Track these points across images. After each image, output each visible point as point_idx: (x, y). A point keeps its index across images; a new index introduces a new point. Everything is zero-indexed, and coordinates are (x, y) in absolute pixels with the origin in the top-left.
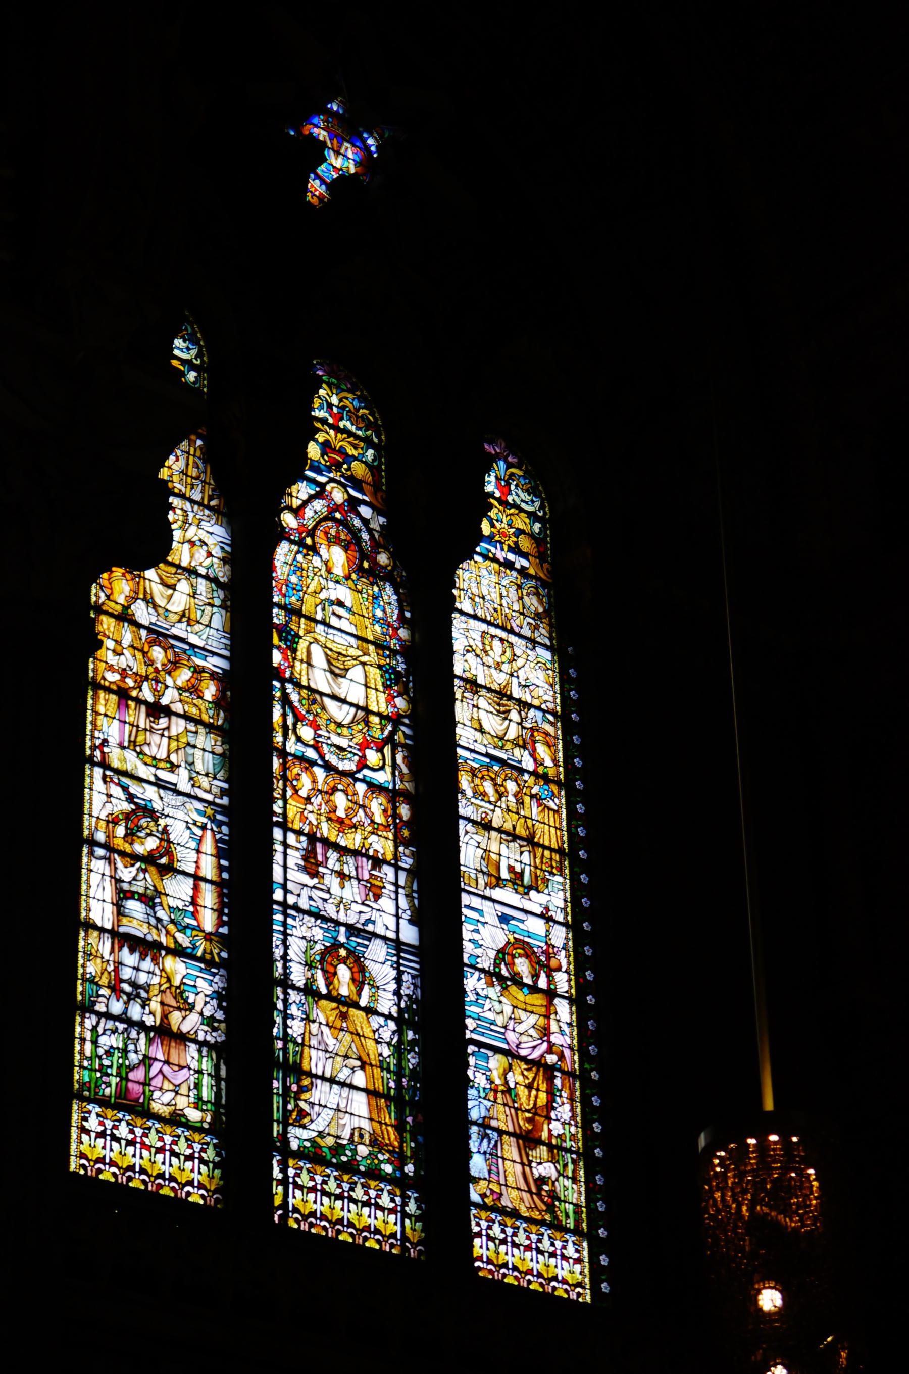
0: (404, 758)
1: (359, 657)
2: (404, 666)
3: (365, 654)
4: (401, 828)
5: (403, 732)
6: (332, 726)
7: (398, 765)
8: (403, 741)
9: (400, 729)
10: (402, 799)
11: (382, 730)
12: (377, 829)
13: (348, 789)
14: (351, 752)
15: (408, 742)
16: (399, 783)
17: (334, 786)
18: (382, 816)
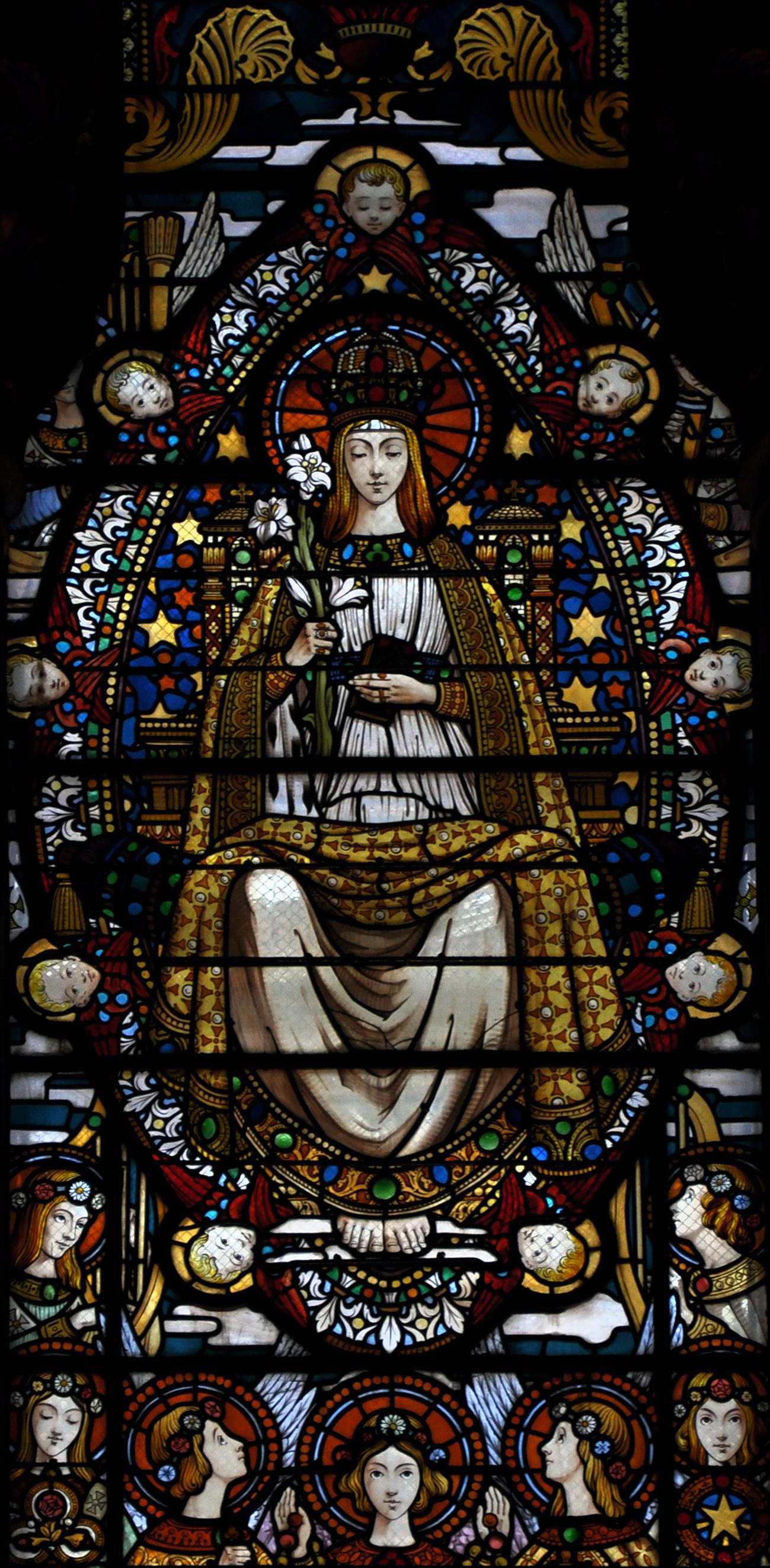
0: (710, 1209)
1: (484, 847)
2: (714, 813)
3: (510, 830)
4: (699, 1505)
5: (711, 1096)
6: (352, 1183)
7: (687, 1242)
8: (707, 1129)
9: (694, 1087)
10: (700, 1380)
11: (601, 1122)
12: (575, 1547)
13: (433, 1420)
14: (440, 1264)
15: (734, 1129)
16: (687, 1315)
17: (360, 1429)
18: (602, 1486)
